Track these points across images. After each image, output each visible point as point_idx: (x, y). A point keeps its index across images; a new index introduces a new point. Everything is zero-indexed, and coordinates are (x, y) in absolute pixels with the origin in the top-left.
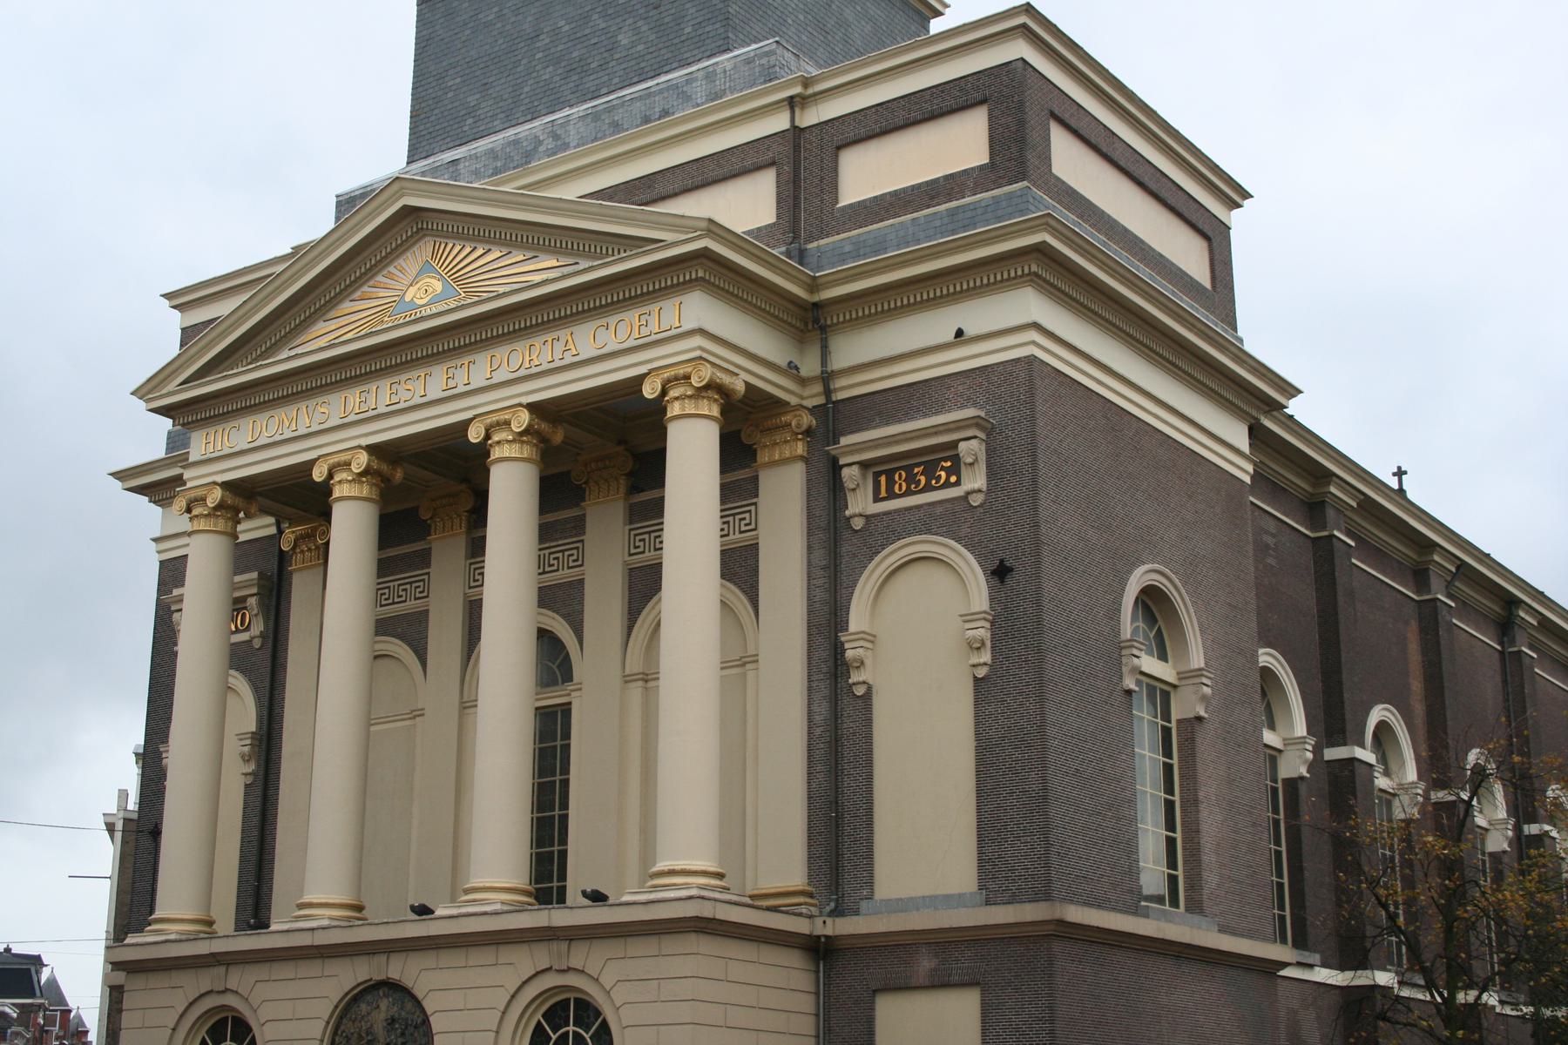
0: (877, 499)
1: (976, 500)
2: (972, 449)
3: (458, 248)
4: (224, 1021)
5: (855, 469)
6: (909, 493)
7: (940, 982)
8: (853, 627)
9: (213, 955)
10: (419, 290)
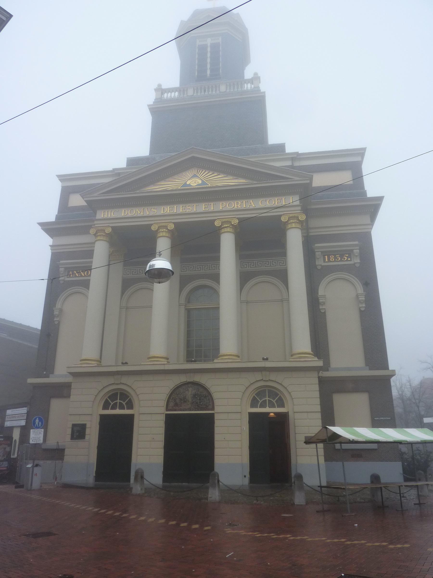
0: (324, 261)
1: (357, 265)
2: (356, 251)
3: (203, 172)
4: (117, 393)
5: (320, 253)
6: (335, 261)
7: (356, 390)
8: (320, 294)
9: (117, 371)
10: (193, 180)
